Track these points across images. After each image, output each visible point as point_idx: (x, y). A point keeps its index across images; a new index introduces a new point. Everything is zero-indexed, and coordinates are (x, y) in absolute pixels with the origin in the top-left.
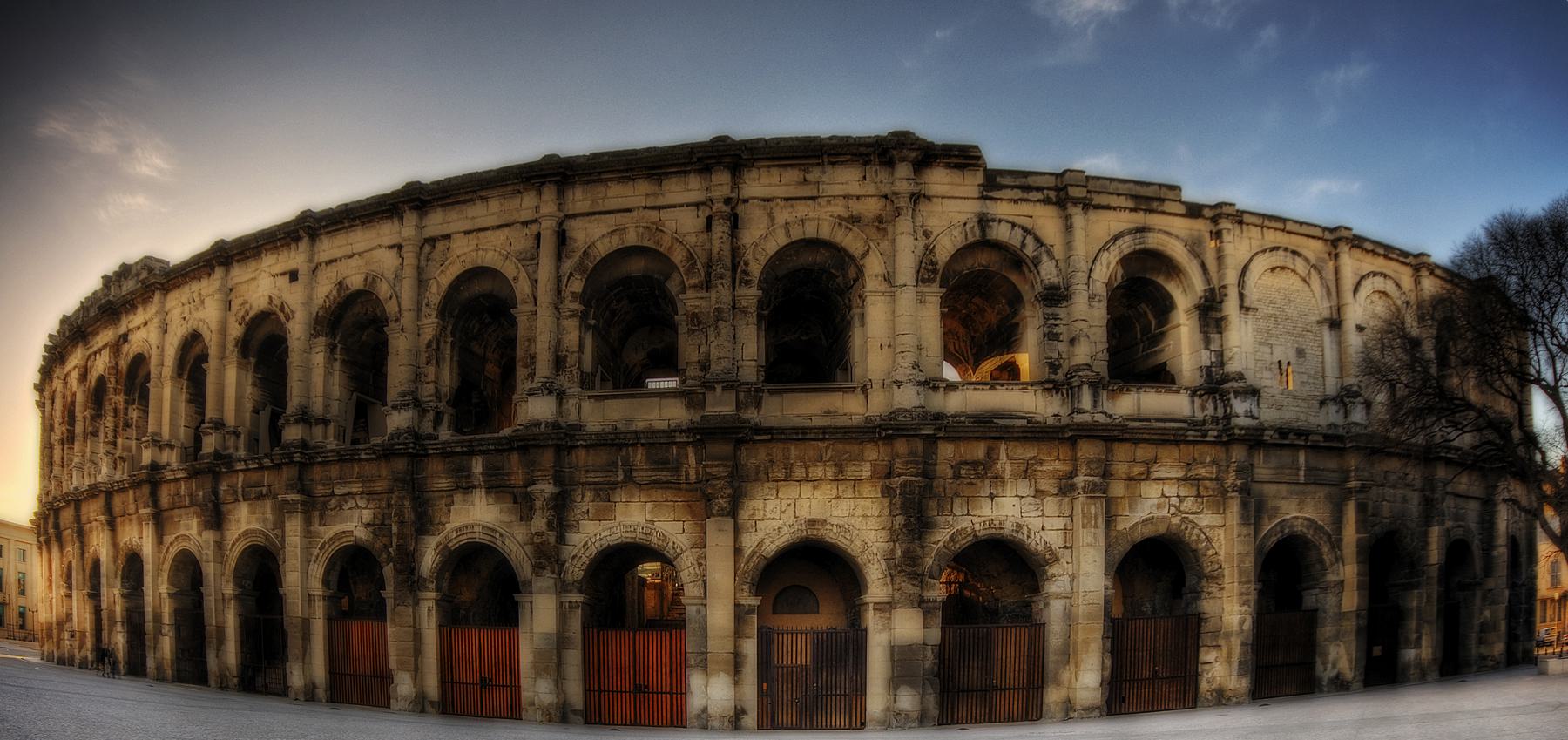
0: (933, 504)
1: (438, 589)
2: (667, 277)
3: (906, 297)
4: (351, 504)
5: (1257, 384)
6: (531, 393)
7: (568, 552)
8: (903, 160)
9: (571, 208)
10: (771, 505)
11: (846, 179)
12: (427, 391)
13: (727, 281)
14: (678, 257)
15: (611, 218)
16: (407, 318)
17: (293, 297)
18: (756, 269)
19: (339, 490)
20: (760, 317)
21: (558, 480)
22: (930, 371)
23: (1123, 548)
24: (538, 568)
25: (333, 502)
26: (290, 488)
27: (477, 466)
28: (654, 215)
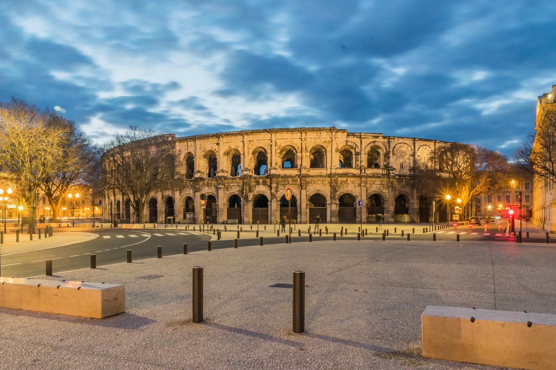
7: (277, 195)
14: (296, 147)
18: (309, 150)
24: (272, 199)
27: (261, 181)
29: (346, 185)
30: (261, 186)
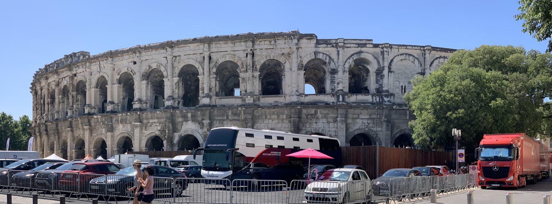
0: (301, 124)
1: (178, 146)
3: (294, 74)
4: (155, 125)
5: (394, 92)
6: (203, 97)
8: (294, 38)
9: (212, 50)
10: (262, 125)
11: (281, 43)
12: (176, 96)
13: (251, 70)
14: (239, 64)
16: (169, 77)
17: (135, 68)
18: (258, 67)
19: (151, 121)
20: (260, 79)
21: (210, 119)
22: (301, 92)
25: (149, 124)
26: (136, 121)
27: (189, 115)
28: (233, 53)
29: (314, 121)
30: (190, 122)
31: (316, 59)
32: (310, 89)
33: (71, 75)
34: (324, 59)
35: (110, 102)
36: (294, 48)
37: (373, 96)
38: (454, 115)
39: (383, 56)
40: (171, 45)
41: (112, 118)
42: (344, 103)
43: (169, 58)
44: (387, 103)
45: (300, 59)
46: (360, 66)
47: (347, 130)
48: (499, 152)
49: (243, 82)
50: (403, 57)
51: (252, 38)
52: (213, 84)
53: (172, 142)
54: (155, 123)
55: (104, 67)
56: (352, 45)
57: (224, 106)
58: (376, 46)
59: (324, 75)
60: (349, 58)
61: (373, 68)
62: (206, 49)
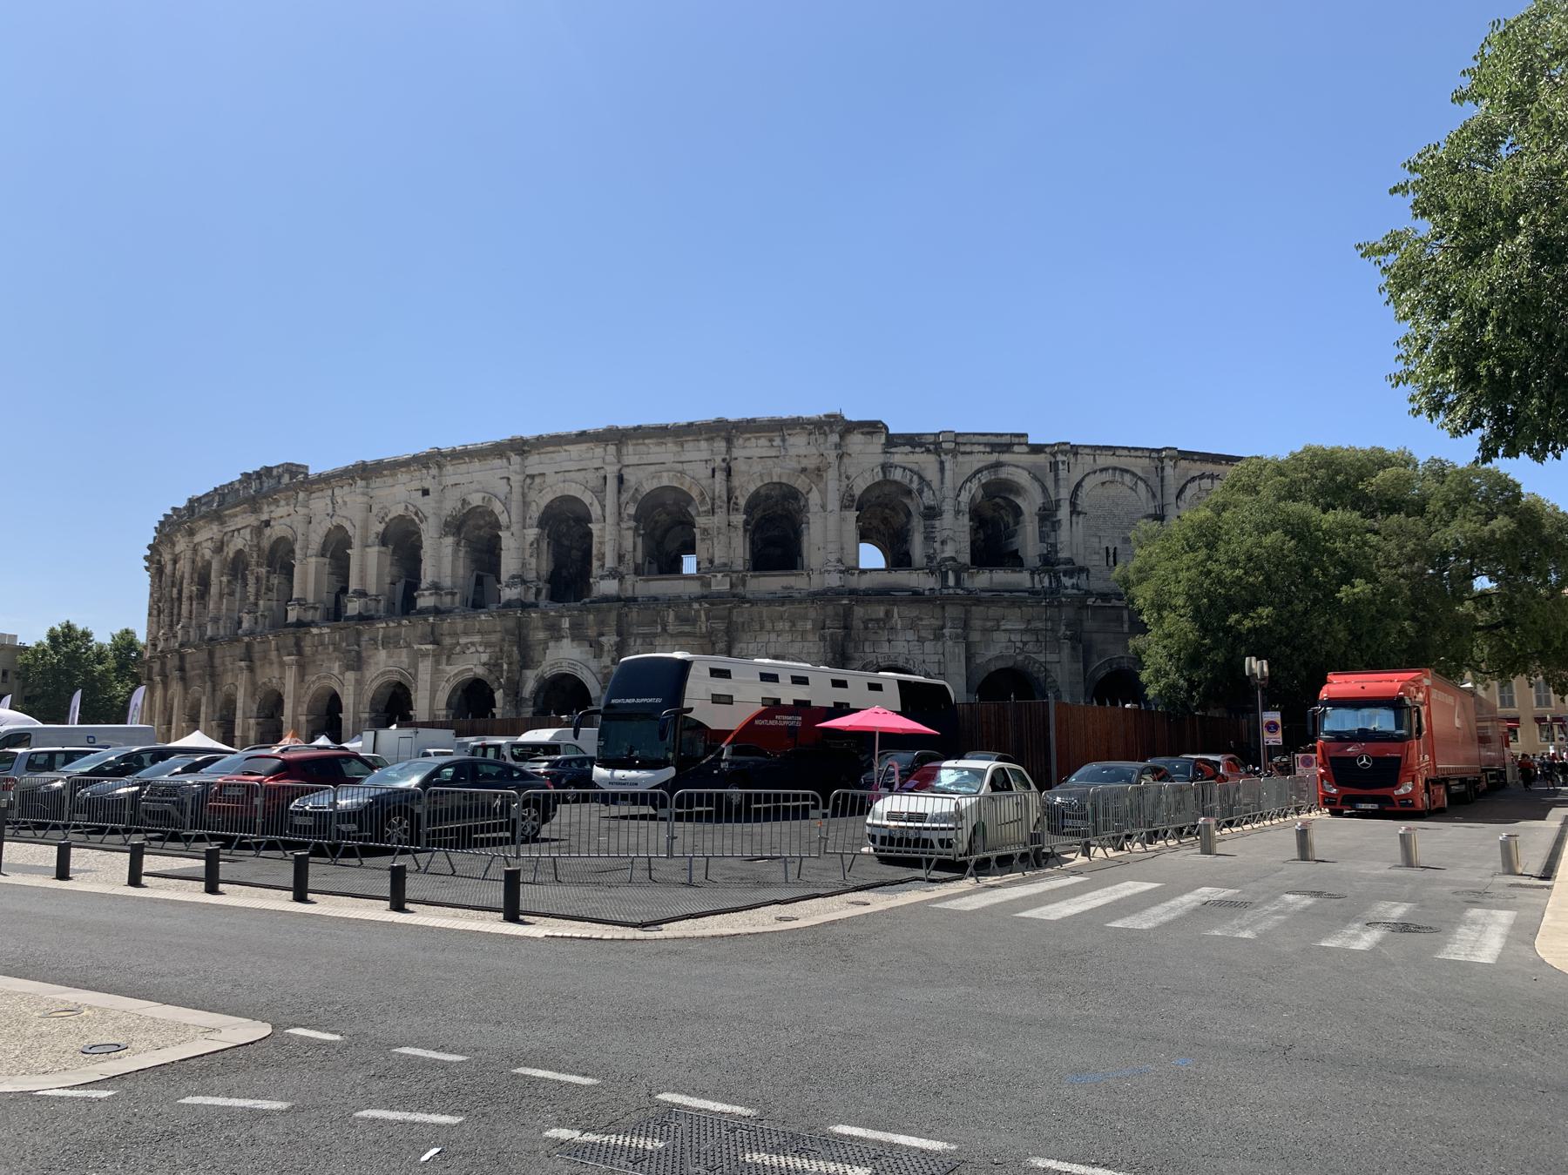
2: (689, 504)
3: (833, 520)
4: (473, 649)
6: (602, 578)
9: (627, 460)
11: (799, 443)
12: (531, 575)
13: (724, 509)
14: (694, 494)
15: (652, 468)
17: (427, 505)
18: (742, 502)
19: (463, 640)
20: (745, 531)
21: (619, 634)
23: (980, 677)
25: (458, 649)
27: (566, 623)
29: (884, 635)
30: (566, 642)
31: (886, 481)
32: (871, 557)
33: (256, 523)
34: (906, 481)
35: (355, 591)
36: (832, 455)
37: (1032, 573)
38: (1248, 623)
39: (1056, 475)
40: (520, 447)
41: (359, 633)
42: (960, 591)
43: (516, 479)
44: (1069, 591)
45: (845, 482)
46: (998, 500)
47: (969, 658)
48: (1371, 718)
49: (703, 540)
50: (1106, 476)
51: (726, 431)
52: (628, 543)
53: (517, 694)
54: (473, 644)
55: (345, 503)
56: (976, 448)
57: (656, 599)
58: (1037, 449)
59: (908, 522)
60: (969, 480)
61: (1030, 504)
62: (611, 458)
